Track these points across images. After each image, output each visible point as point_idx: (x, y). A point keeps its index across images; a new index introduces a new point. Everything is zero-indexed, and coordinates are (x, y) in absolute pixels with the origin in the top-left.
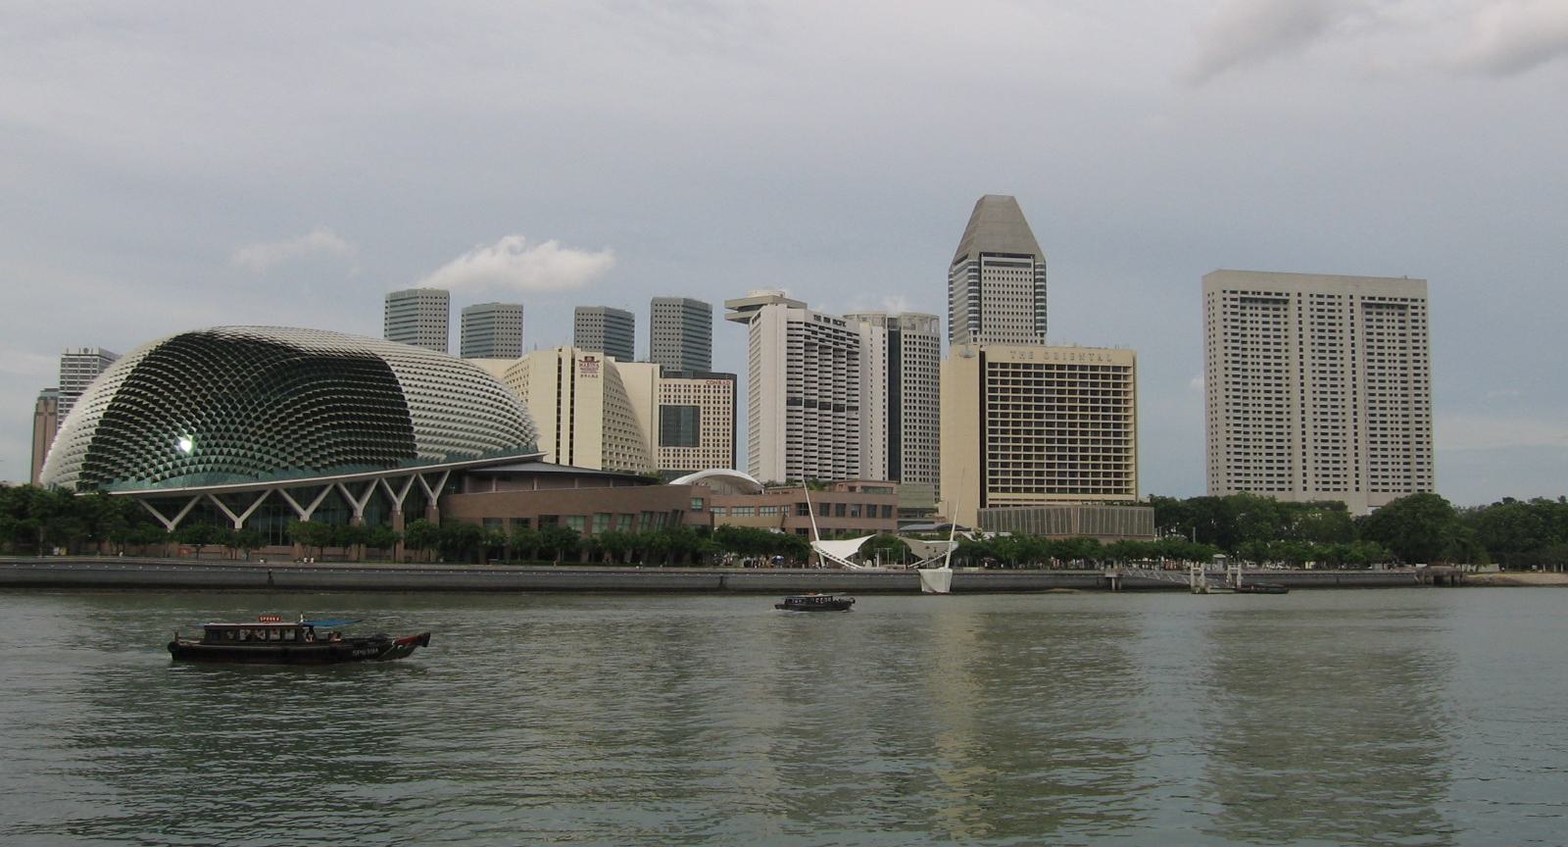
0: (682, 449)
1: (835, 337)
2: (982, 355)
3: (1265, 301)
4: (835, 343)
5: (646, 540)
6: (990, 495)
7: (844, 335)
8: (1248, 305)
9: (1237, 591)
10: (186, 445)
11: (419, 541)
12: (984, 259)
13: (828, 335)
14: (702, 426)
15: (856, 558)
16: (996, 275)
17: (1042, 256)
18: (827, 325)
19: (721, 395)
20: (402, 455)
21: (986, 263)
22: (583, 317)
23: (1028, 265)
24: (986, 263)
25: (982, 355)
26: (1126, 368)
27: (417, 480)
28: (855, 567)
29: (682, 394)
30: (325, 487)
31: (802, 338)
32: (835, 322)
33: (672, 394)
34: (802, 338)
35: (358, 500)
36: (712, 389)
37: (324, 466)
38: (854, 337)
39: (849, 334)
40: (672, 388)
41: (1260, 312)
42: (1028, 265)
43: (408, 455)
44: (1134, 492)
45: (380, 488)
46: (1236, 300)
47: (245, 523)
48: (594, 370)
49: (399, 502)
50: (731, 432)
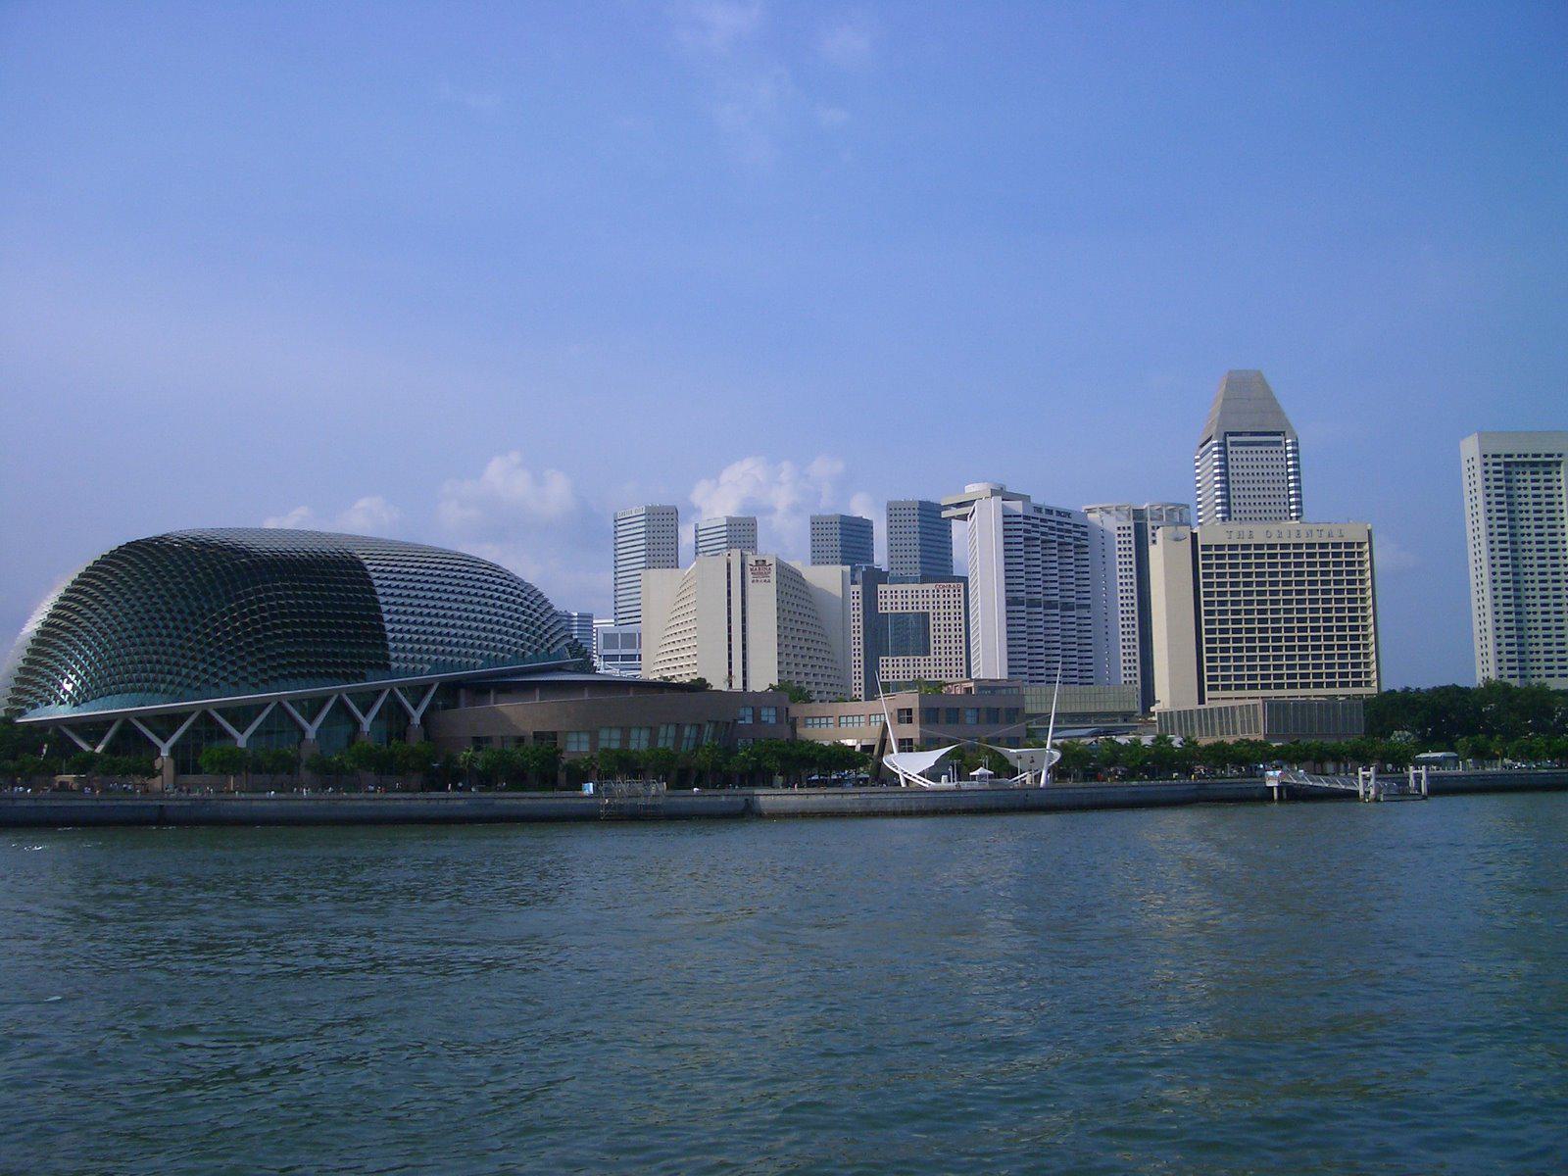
0: (911, 658)
1: (1059, 530)
2: (1194, 536)
3: (1533, 464)
4: (1060, 537)
5: (723, 759)
6: (1207, 694)
7: (1066, 527)
8: (1514, 469)
9: (1425, 798)
11: (384, 766)
12: (1230, 439)
13: (1052, 528)
14: (932, 633)
15: (933, 774)
16: (1244, 456)
18: (1048, 517)
19: (952, 599)
20: (370, 666)
21: (1233, 444)
22: (818, 525)
23: (1279, 443)
24: (1233, 444)
25: (1194, 536)
26: (1360, 545)
27: (392, 692)
28: (928, 784)
29: (910, 600)
30: (268, 704)
31: (1021, 533)
32: (1059, 513)
33: (920, 600)
34: (1021, 533)
35: (310, 723)
36: (941, 594)
37: (263, 681)
38: (1082, 529)
39: (1075, 526)
40: (899, 594)
41: (1528, 477)
42: (1279, 443)
43: (378, 666)
44: (1375, 684)
45: (340, 702)
46: (1498, 464)
47: (173, 750)
48: (767, 575)
49: (366, 723)
50: (963, 639)
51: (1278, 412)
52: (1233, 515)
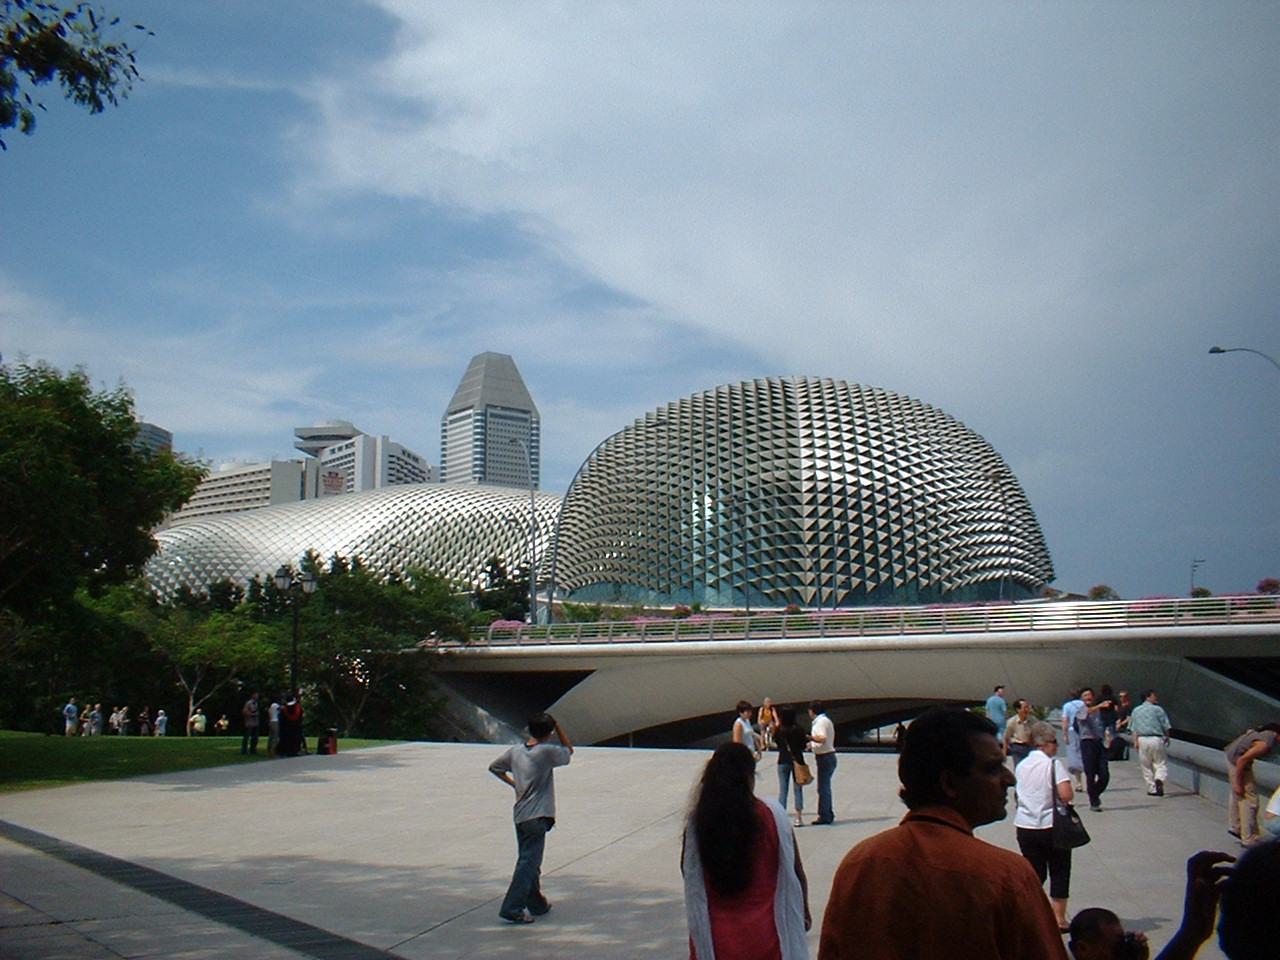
1: (414, 473)
7: (417, 471)
10: (87, 554)
12: (490, 411)
17: (537, 412)
21: (492, 415)
24: (492, 415)
39: (421, 471)
42: (526, 420)
51: (524, 392)
52: (488, 477)
